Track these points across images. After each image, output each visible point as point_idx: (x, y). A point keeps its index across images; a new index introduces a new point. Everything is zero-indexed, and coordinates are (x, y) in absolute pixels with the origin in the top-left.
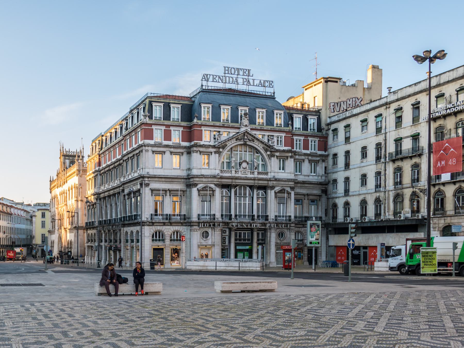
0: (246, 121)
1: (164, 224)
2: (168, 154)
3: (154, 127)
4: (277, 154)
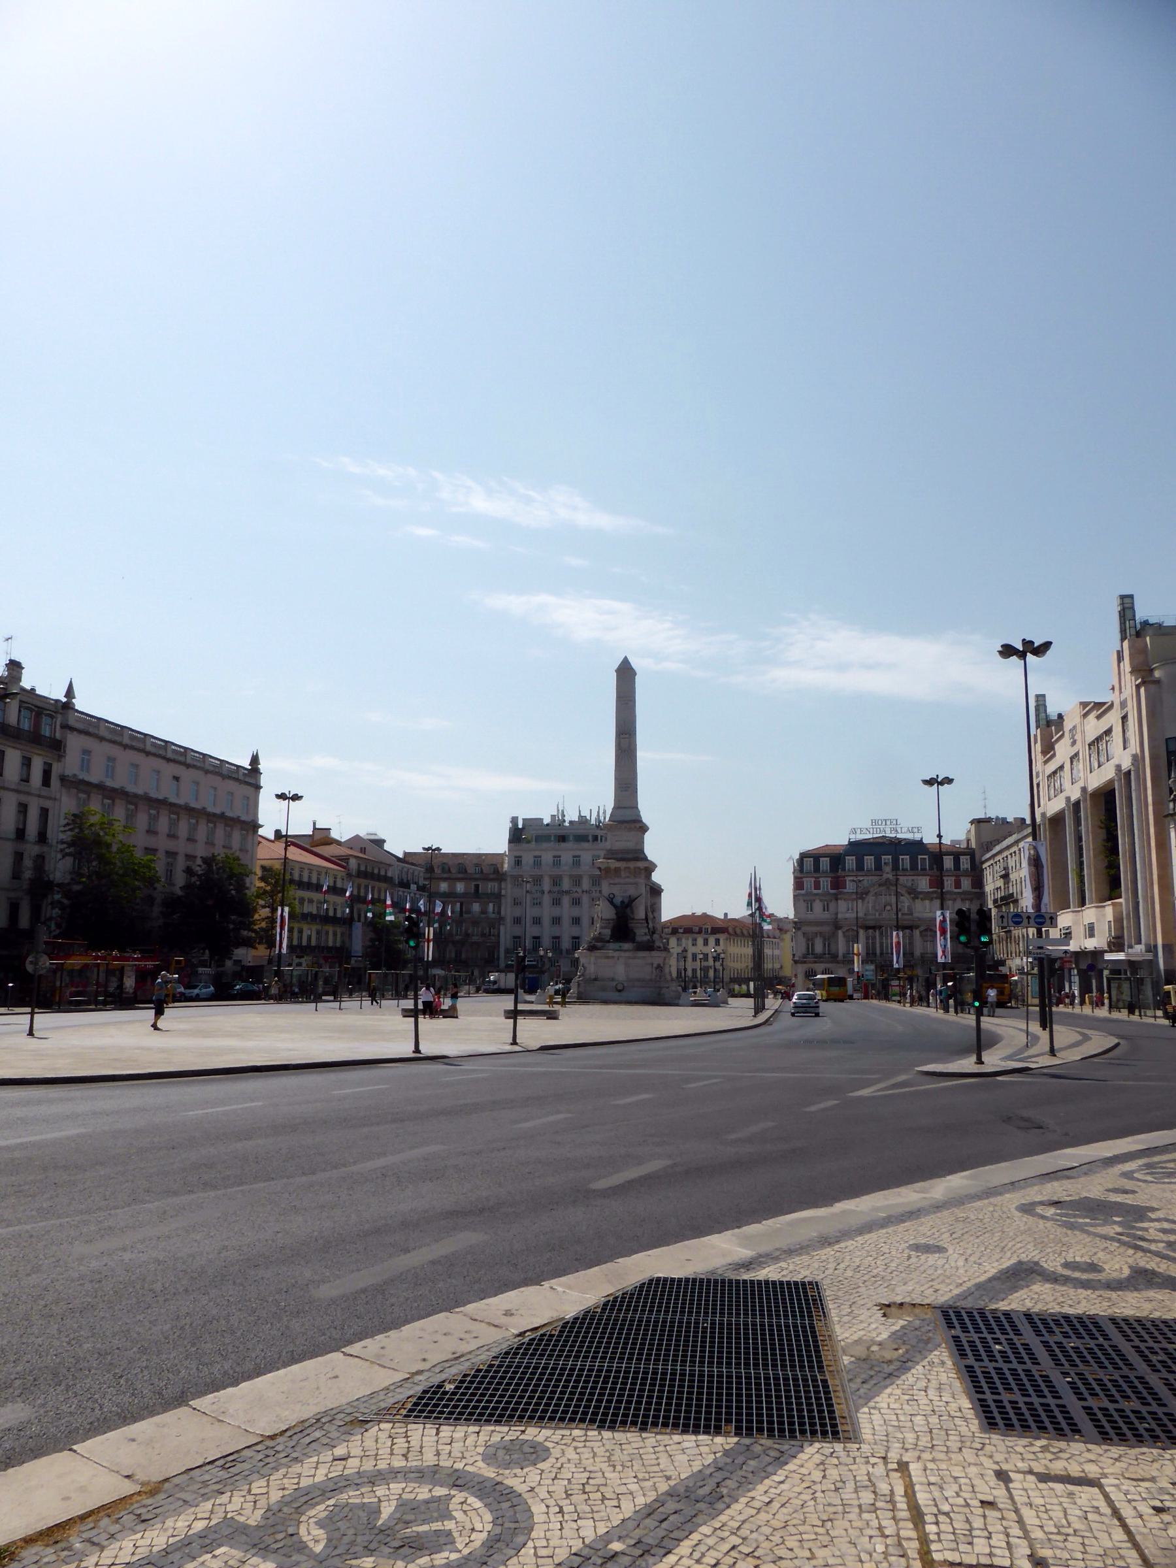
0: (888, 869)
1: (815, 962)
2: (818, 901)
3: (805, 879)
4: (921, 896)
